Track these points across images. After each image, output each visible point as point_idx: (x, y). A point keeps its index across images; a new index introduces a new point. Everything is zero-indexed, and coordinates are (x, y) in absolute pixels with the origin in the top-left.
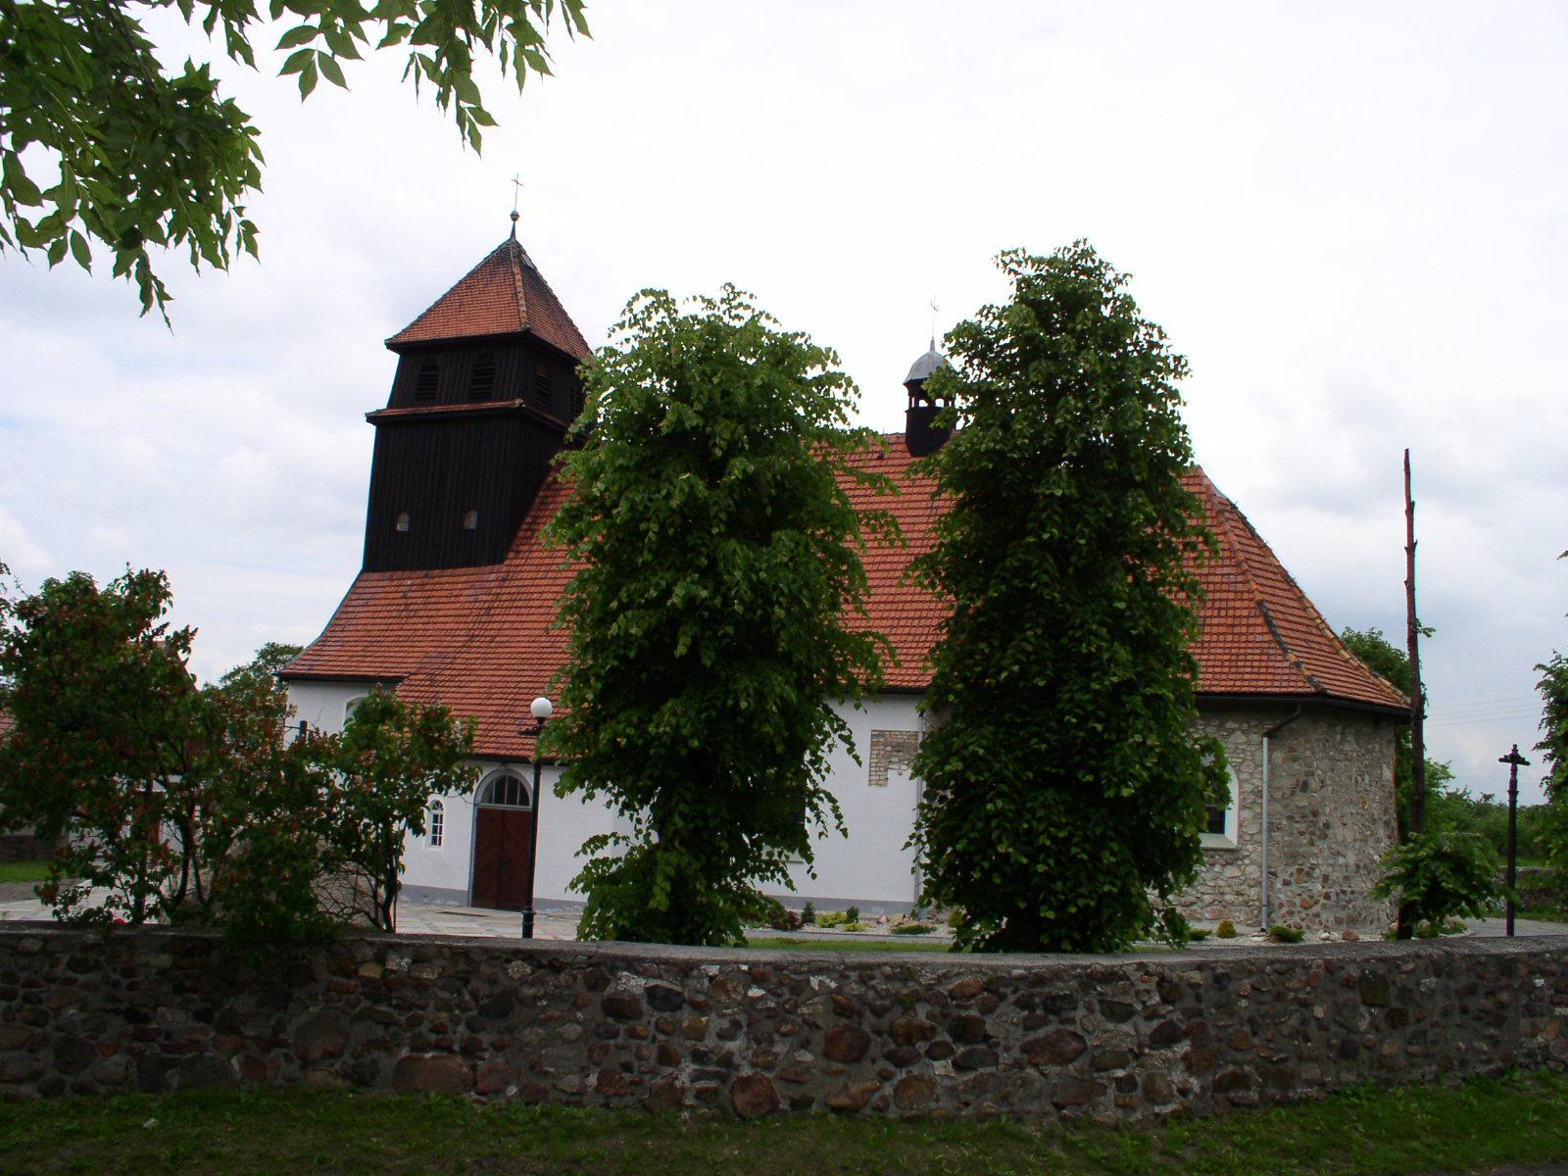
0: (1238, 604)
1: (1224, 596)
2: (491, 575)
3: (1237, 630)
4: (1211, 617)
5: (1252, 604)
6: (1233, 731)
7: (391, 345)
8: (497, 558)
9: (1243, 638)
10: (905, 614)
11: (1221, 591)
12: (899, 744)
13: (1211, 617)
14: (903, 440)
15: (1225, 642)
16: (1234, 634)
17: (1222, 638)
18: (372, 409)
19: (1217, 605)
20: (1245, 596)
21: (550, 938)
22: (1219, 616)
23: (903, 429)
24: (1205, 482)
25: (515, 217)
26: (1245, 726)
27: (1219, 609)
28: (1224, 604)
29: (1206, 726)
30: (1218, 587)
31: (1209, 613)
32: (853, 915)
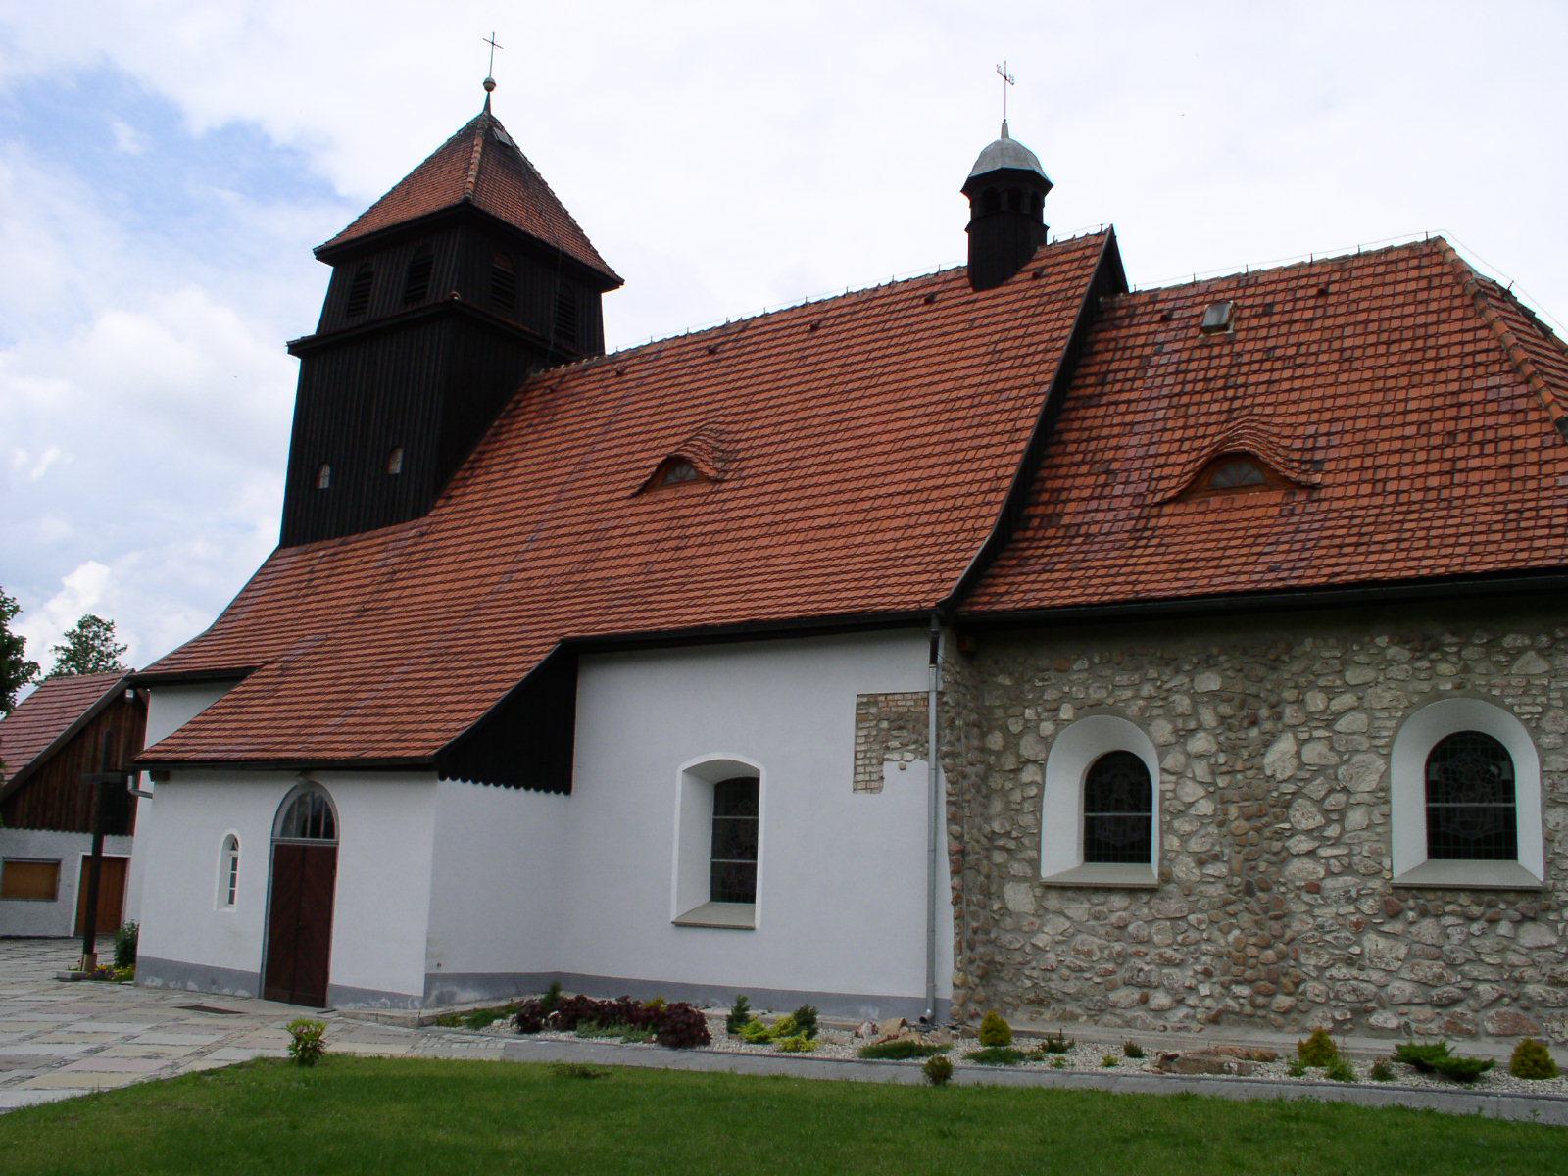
0: (1518, 431)
1: (1490, 421)
2: (409, 531)
3: (1517, 473)
4: (1466, 458)
5: (1546, 428)
6: (1521, 651)
7: (324, 254)
8: (420, 511)
9: (1532, 484)
10: (929, 507)
11: (1484, 414)
12: (900, 717)
13: (1466, 458)
14: (965, 273)
15: (1495, 494)
16: (1511, 480)
17: (1487, 489)
18: (296, 336)
19: (1478, 436)
20: (1533, 416)
21: (87, 1092)
22: (1481, 455)
23: (964, 261)
24: (1450, 257)
25: (489, 86)
26: (1544, 640)
27: (1481, 444)
28: (1490, 435)
29: (1462, 646)
30: (1478, 409)
31: (1462, 451)
32: (806, 1021)
